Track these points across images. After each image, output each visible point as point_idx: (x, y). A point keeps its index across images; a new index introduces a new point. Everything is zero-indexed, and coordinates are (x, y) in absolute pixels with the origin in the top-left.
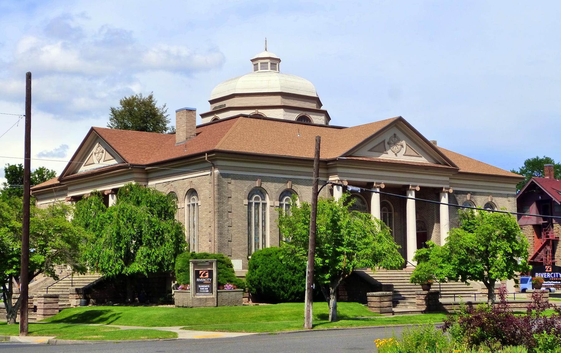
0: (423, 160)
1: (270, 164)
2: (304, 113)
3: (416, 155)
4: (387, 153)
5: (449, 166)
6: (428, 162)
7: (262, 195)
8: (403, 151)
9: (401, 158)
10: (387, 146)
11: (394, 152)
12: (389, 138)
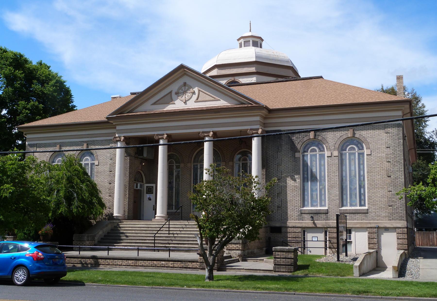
0: (222, 103)
1: (53, 133)
2: (232, 79)
3: (212, 99)
4: (174, 104)
5: (251, 104)
6: (229, 104)
7: (92, 156)
8: (195, 97)
9: (192, 105)
10: (174, 95)
11: (183, 101)
12: (177, 88)
